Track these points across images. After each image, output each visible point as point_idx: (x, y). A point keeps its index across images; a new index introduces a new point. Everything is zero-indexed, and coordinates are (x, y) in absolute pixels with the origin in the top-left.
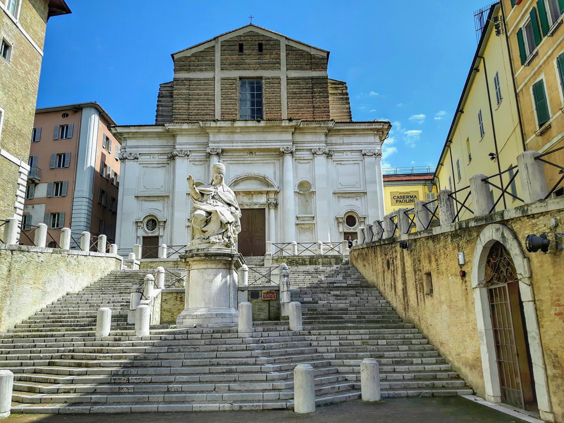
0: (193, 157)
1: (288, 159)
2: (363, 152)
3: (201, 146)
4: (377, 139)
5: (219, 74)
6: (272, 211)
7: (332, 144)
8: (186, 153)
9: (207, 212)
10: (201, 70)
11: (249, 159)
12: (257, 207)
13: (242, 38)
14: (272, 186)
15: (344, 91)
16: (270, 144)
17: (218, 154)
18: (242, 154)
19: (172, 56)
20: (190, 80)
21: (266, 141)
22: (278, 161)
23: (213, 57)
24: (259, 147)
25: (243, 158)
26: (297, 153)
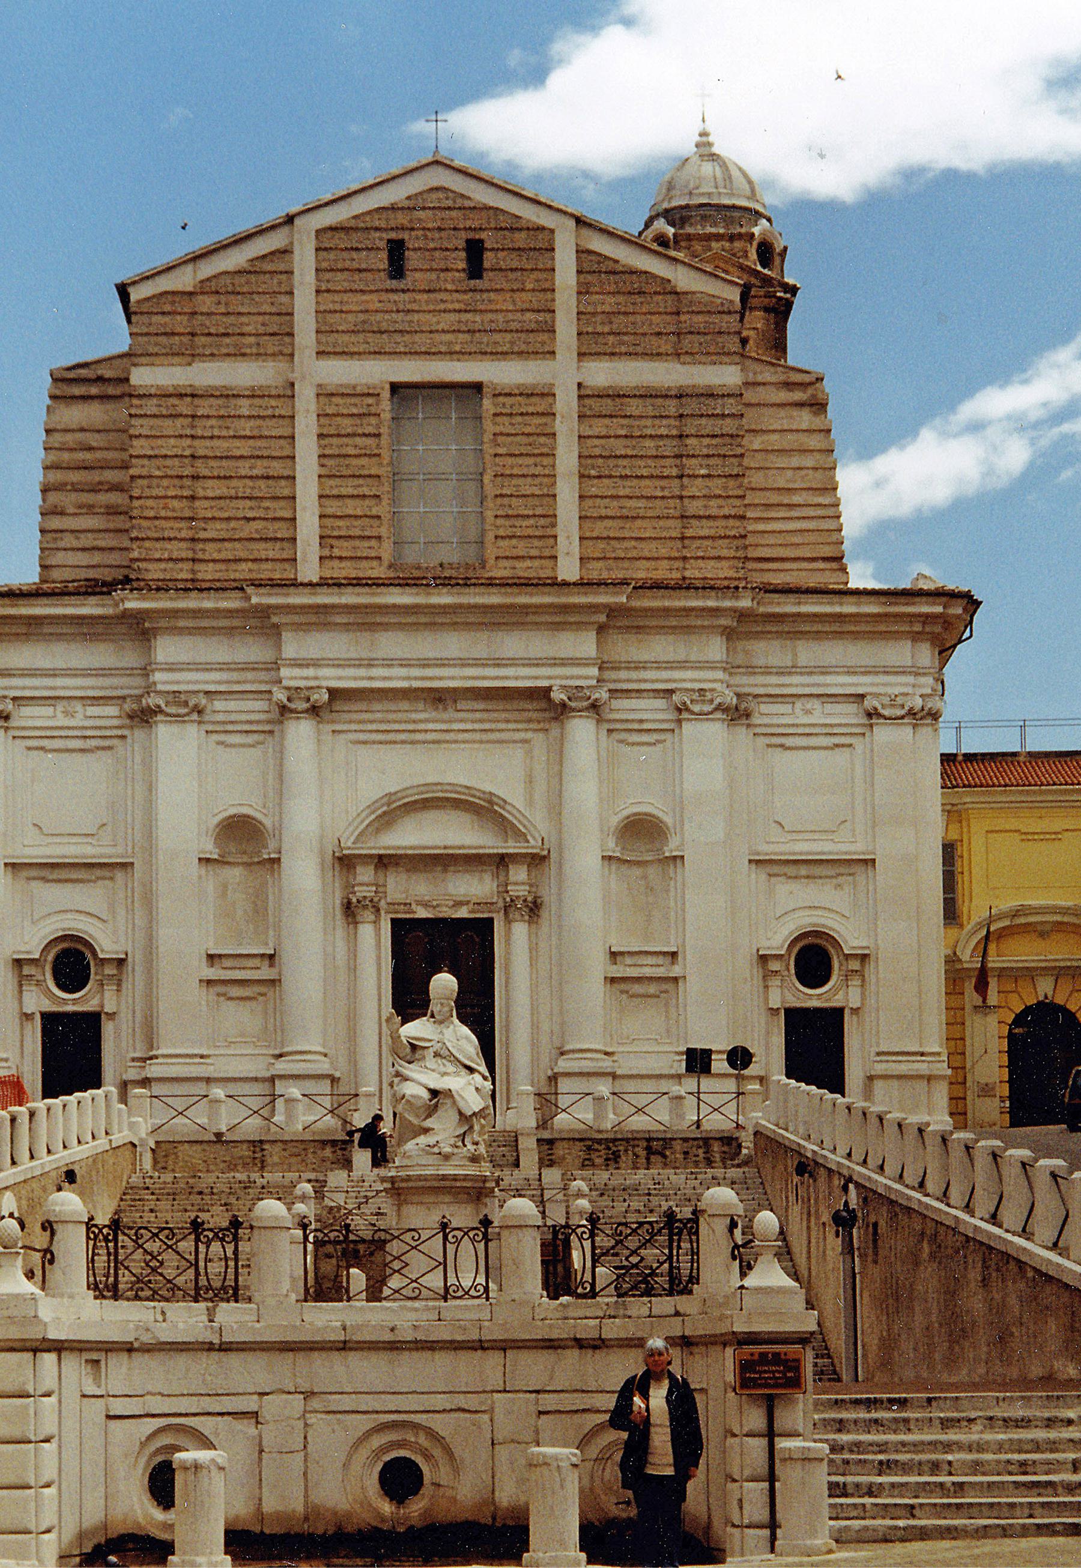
1: (582, 731)
2: (869, 703)
3: (250, 675)
4: (926, 655)
7: (751, 670)
9: (429, 1090)
11: (430, 726)
12: (463, 913)
13: (402, 219)
16: (510, 671)
17: (314, 710)
18: (405, 705)
19: (123, 291)
21: (498, 663)
22: (541, 735)
23: (284, 299)
26: (616, 704)
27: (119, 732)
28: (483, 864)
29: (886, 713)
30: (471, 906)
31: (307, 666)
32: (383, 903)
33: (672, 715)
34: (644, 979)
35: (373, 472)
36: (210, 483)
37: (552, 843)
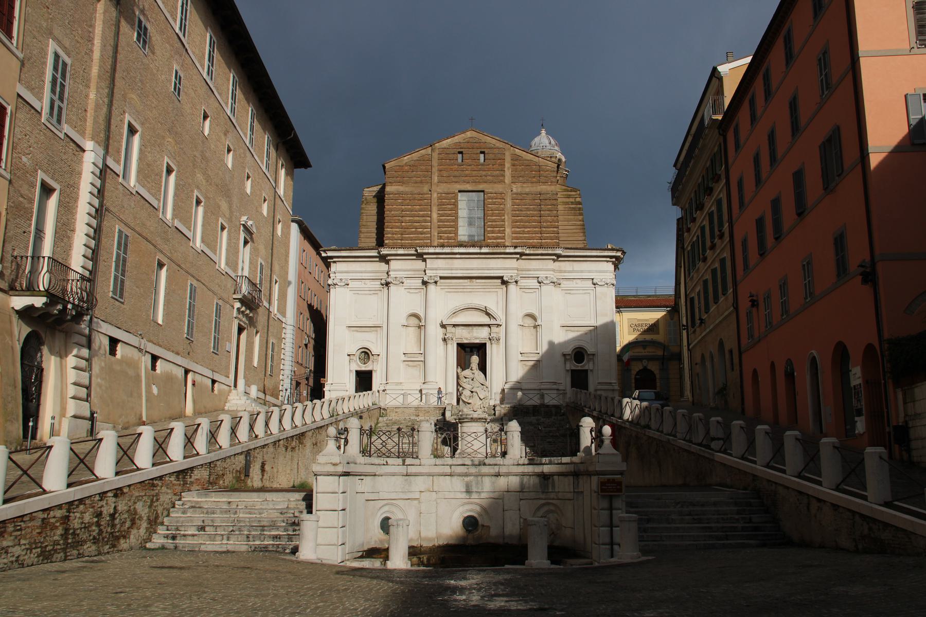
1: (512, 287)
2: (595, 281)
6: (494, 346)
12: (477, 341)
13: (462, 145)
15: (578, 200)
37: (503, 322)
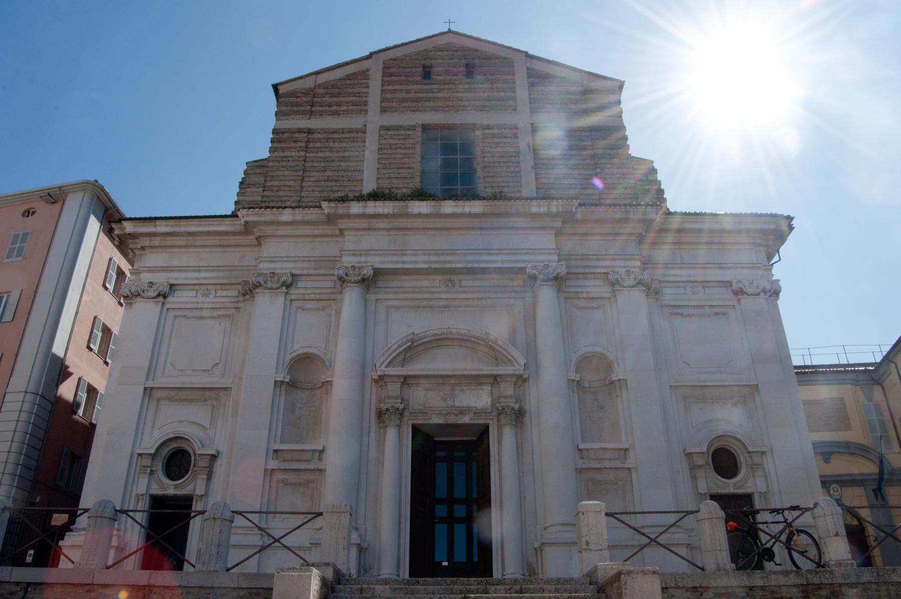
0: (302, 291)
2: (735, 287)
5: (374, 119)
8: (282, 280)
10: (337, 113)
12: (466, 420)
14: (509, 361)
15: (650, 178)
16: (499, 258)
19: (275, 87)
20: (309, 131)
24: (470, 265)
25: (429, 292)
27: (236, 305)
28: (481, 384)
29: (749, 291)
30: (472, 414)
31: (361, 255)
32: (406, 414)
33: (609, 289)
34: (597, 474)
35: (410, 166)
36: (314, 174)
